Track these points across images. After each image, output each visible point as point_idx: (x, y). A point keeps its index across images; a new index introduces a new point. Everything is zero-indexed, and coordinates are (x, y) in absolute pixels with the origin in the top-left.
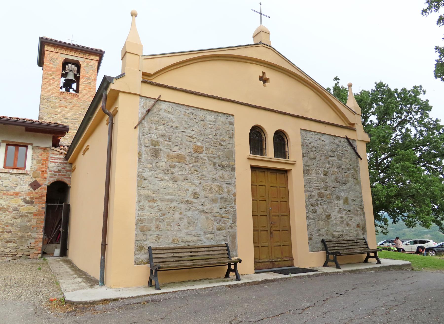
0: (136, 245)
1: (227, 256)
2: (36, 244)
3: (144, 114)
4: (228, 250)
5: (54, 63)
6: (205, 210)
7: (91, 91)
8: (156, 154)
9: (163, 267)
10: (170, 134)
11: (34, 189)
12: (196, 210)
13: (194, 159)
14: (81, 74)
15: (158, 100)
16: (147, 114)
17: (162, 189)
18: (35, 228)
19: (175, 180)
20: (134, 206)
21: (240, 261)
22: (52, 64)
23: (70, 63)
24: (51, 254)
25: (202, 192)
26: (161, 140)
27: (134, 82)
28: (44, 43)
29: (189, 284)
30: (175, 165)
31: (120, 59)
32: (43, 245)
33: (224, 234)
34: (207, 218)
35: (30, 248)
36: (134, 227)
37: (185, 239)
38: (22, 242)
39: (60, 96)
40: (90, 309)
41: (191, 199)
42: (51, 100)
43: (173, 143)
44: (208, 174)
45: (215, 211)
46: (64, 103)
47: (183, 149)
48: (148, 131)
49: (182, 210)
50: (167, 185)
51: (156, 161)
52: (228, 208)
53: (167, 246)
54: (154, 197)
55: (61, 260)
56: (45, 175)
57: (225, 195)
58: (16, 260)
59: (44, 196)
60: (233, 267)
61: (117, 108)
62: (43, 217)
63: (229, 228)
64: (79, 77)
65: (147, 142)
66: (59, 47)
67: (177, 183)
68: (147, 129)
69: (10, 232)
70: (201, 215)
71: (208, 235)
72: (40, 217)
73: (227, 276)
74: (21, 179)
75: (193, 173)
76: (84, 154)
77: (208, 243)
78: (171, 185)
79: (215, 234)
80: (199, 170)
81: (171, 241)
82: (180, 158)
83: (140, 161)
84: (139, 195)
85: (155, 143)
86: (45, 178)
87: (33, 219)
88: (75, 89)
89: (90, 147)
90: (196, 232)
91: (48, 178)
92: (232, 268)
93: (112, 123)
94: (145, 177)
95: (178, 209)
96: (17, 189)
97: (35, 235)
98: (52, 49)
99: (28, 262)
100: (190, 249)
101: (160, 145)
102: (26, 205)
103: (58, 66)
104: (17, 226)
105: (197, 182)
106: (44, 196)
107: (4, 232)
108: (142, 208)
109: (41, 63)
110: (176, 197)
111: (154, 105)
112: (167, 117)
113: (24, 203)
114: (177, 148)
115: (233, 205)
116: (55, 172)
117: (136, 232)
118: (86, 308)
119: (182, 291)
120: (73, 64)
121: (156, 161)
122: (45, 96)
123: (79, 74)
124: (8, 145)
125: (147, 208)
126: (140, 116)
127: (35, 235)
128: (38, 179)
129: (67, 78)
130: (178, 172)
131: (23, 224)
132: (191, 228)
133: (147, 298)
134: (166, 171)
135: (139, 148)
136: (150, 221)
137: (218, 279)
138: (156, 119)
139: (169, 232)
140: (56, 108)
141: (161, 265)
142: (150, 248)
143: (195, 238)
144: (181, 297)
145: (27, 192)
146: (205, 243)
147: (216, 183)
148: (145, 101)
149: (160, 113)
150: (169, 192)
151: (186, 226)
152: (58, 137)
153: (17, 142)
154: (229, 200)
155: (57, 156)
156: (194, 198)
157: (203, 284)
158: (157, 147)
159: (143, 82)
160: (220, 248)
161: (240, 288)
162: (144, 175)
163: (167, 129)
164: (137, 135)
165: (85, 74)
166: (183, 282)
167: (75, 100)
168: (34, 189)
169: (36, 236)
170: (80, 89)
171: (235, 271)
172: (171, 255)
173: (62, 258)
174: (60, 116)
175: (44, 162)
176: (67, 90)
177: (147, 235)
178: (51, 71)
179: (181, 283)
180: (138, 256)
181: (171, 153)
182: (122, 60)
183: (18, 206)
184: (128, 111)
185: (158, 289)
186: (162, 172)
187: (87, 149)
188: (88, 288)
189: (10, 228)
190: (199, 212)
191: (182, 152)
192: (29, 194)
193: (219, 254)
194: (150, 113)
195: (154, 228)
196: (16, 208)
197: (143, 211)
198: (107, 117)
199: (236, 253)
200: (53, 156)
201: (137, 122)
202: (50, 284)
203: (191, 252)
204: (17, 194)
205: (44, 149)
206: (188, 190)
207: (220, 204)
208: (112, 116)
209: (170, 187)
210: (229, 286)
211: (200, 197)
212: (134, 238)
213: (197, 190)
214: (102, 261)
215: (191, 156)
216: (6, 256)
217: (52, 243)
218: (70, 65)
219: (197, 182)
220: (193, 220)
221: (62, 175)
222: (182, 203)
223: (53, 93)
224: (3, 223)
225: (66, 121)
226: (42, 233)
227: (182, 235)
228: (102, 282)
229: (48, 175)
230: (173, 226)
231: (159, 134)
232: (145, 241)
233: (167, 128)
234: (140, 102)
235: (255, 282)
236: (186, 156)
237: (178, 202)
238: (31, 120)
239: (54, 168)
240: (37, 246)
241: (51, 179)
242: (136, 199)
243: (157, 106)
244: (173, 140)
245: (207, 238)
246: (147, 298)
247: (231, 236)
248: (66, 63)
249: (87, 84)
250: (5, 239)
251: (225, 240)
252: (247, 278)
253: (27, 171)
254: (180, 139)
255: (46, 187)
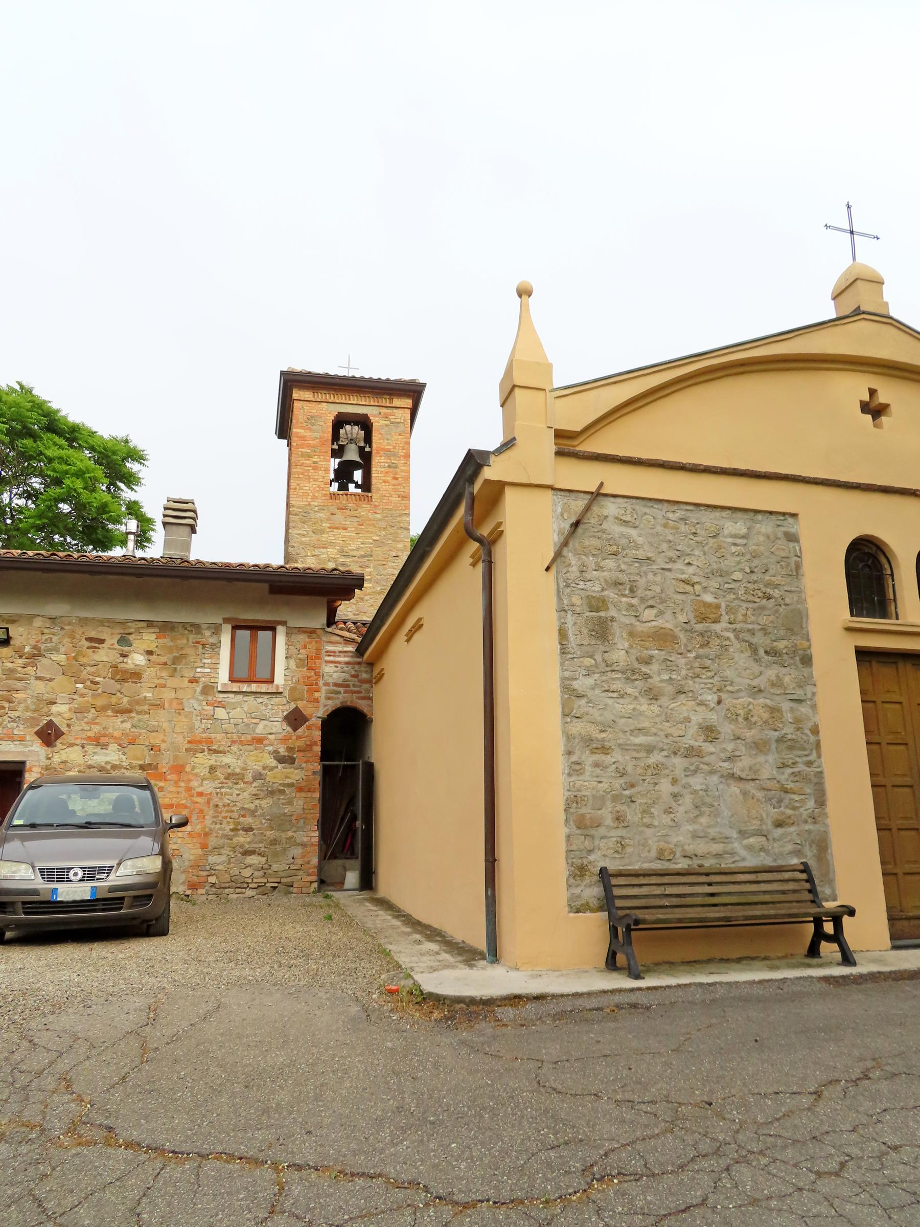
0: (570, 861)
1: (810, 897)
2: (306, 860)
3: (566, 533)
4: (810, 880)
5: (314, 428)
6: (739, 773)
7: (399, 484)
8: (601, 631)
9: (643, 920)
10: (633, 578)
11: (295, 730)
12: (712, 772)
13: (699, 639)
14: (374, 446)
15: (597, 495)
16: (574, 532)
17: (623, 720)
18: (302, 821)
19: (653, 695)
20: (558, 764)
21: (851, 912)
22: (309, 429)
23: (349, 423)
24: (339, 884)
25: (726, 723)
26: (610, 594)
27: (537, 458)
28: (291, 382)
29: (712, 967)
30: (651, 657)
31: (499, 404)
32: (319, 862)
33: (794, 836)
34: (745, 794)
35: (292, 867)
36: (562, 816)
37: (690, 849)
38: (276, 854)
39: (330, 503)
40: (486, 1017)
41: (697, 744)
42: (312, 515)
43: (642, 600)
44: (739, 676)
45: (765, 774)
46: (339, 518)
47: (668, 615)
48: (578, 574)
49: (677, 772)
50: (634, 709)
51: (602, 648)
52: (801, 767)
53: (646, 866)
54: (603, 740)
55: (366, 899)
56: (316, 695)
57: (789, 730)
58: (265, 897)
59: (315, 743)
60: (829, 928)
61: (500, 524)
62: (317, 795)
63: (806, 822)
64: (370, 453)
65: (579, 602)
66: (323, 389)
67: (659, 702)
68: (574, 569)
69: (251, 829)
70: (728, 785)
71: (752, 840)
72: (309, 794)
73: (813, 951)
74: (266, 705)
75: (698, 676)
76: (408, 641)
77: (752, 861)
78: (644, 708)
79: (770, 837)
80: (714, 667)
81: (654, 854)
82: (663, 638)
83: (564, 651)
84: (569, 737)
85: (597, 604)
86: (317, 701)
87: (295, 800)
88: (360, 483)
89: (425, 622)
90: (717, 829)
91: (323, 700)
92: (826, 930)
93: (490, 562)
94: (580, 690)
95: (667, 771)
96: (260, 729)
97: (301, 837)
98: (307, 395)
99: (291, 901)
100: (707, 874)
101: (610, 606)
102: (280, 766)
103: (323, 432)
104: (263, 815)
105: (710, 697)
106: (315, 743)
107: (238, 830)
108: (575, 769)
109: (284, 430)
110: (658, 739)
111: (588, 508)
112: (622, 535)
113: (274, 763)
114: (654, 612)
115: (813, 757)
116: (336, 685)
117: (567, 830)
118: (475, 1012)
119: (701, 985)
120: (356, 423)
121: (602, 648)
122: (298, 507)
123: (370, 446)
124: (235, 628)
125: (588, 768)
126: (556, 538)
127: (301, 837)
128: (300, 704)
129: (345, 458)
130: (659, 674)
131: (275, 810)
132: (704, 820)
133: (617, 998)
134: (629, 673)
135: (560, 618)
136: (600, 801)
137: (787, 960)
138: (595, 542)
139: (649, 832)
140: (322, 532)
141: (640, 914)
142: (603, 871)
143: (717, 848)
144: (703, 1001)
145: (280, 736)
146: (743, 859)
147: (762, 700)
148: (565, 501)
149: (605, 526)
150: (640, 726)
151: (692, 816)
152: (334, 601)
153: (253, 621)
154: (802, 745)
155: (340, 648)
156: (705, 741)
157: (751, 970)
158: (602, 614)
159: (559, 453)
160: (787, 875)
161: (863, 987)
162: (576, 685)
163: (623, 567)
164: (554, 587)
165: (385, 445)
166: (695, 962)
167: (364, 509)
168: (295, 730)
169: (305, 839)
170: (374, 481)
171: (837, 937)
172: (658, 891)
173: (365, 894)
174: (332, 551)
175: (311, 664)
176: (343, 487)
177: (593, 837)
178: (308, 446)
179: (691, 964)
180: (577, 891)
181: (640, 627)
182: (502, 406)
183: (264, 768)
184: (528, 528)
185: (638, 977)
186: (619, 675)
187: (418, 626)
188: (461, 966)
189: (248, 820)
190: (722, 776)
191: (666, 622)
192: (285, 740)
193: (783, 892)
194: (580, 530)
195: (609, 821)
196: (260, 774)
197: (581, 778)
198: (475, 545)
199: (834, 891)
200: (330, 648)
201: (552, 555)
202: (368, 952)
203: (710, 884)
204: (259, 740)
205: (311, 633)
206: (688, 720)
207: (776, 756)
208: (488, 545)
209: (641, 714)
210: (827, 979)
211: (722, 737)
212: (562, 847)
213: (713, 718)
214: (490, 900)
215: (691, 631)
216: (246, 885)
217: (334, 856)
218: (348, 427)
219: (711, 698)
220: (708, 800)
221: (353, 692)
222: (675, 753)
223: (314, 498)
224: (235, 809)
225: (347, 560)
226: (317, 834)
227: (681, 838)
228: (493, 953)
229: (321, 695)
230: (656, 813)
231: (606, 581)
232: (590, 852)
233: (624, 563)
234: (555, 504)
235: (899, 972)
236: (676, 630)
237: (665, 753)
238: (214, 563)
239: (335, 675)
240: (308, 863)
241: (330, 702)
242: (561, 747)
243: (595, 509)
244: (640, 592)
245: (749, 848)
246: (617, 998)
247: (813, 841)
248: (340, 422)
249: (389, 467)
250: (242, 846)
251: (798, 853)
252: (874, 961)
253: (277, 686)
254: (658, 589)
255: (320, 722)
